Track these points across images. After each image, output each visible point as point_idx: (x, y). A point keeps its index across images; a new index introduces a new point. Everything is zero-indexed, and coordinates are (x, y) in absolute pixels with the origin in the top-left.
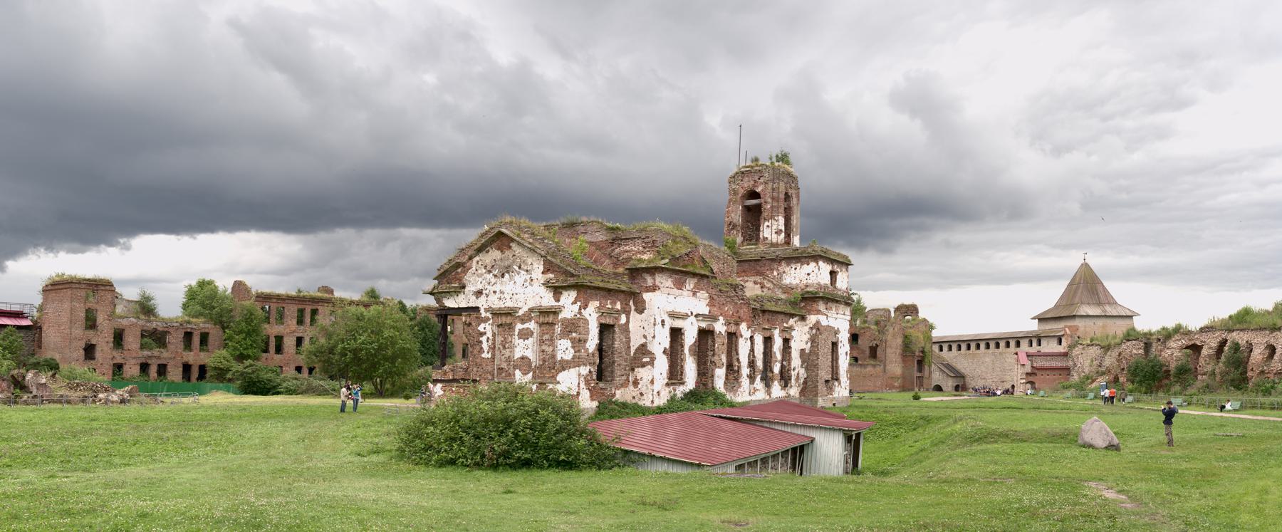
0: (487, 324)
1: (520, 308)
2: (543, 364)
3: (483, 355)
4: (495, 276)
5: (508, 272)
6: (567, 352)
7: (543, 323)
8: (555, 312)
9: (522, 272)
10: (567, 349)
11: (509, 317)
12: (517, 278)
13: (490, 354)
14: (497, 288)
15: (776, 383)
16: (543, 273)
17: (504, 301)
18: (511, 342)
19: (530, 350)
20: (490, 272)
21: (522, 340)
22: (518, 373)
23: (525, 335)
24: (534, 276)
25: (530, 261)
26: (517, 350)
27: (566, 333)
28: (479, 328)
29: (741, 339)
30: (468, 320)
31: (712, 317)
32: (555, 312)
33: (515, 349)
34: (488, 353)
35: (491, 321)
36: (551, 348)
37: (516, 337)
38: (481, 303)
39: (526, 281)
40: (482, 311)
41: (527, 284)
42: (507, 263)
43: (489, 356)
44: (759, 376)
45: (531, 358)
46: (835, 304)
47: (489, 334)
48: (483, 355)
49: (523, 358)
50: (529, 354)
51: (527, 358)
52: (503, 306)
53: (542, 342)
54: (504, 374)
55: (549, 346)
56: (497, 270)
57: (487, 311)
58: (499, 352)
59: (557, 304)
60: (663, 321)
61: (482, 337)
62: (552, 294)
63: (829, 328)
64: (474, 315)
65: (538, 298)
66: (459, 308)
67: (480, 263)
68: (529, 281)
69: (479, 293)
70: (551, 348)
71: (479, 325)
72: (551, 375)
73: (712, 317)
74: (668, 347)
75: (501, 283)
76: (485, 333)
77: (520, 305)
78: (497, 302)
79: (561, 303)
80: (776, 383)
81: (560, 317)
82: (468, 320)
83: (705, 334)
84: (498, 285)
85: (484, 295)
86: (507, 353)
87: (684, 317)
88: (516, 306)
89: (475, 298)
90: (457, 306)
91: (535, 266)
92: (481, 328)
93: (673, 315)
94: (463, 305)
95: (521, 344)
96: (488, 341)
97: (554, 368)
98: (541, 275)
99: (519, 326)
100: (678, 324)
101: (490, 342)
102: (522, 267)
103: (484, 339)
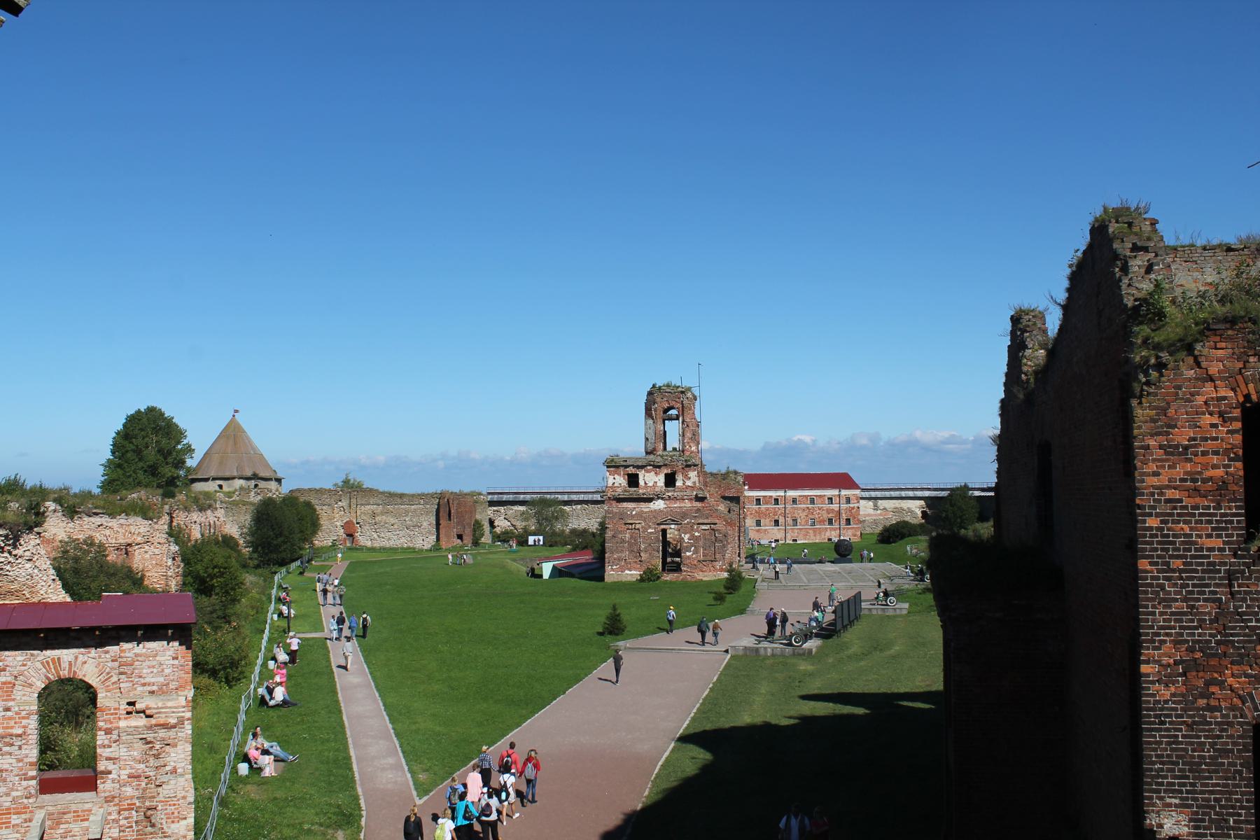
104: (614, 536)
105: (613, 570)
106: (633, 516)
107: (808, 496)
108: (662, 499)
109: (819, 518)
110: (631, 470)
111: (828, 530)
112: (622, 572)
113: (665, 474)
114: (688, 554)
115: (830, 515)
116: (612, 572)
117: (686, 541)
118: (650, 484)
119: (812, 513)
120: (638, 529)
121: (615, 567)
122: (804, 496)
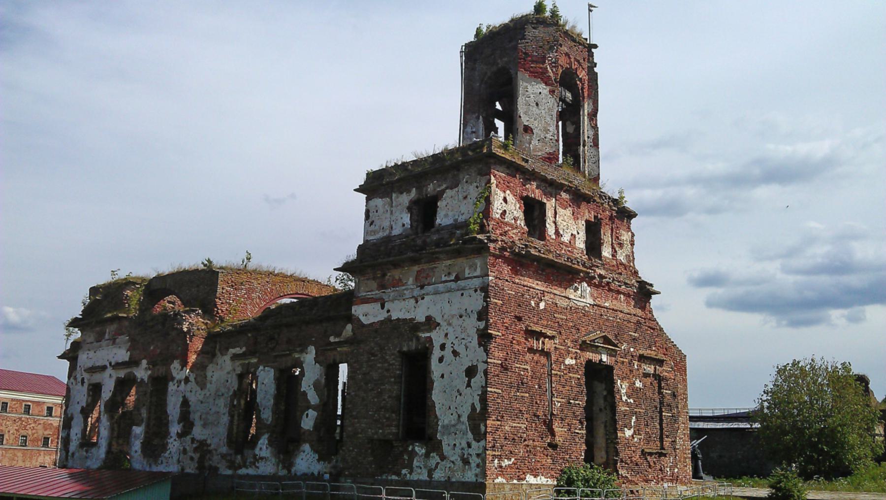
15: (306, 447)
29: (171, 383)
31: (133, 362)
44: (266, 436)
46: (416, 268)
60: (83, 379)
63: (391, 326)
73: (133, 362)
74: (85, 406)
80: (306, 447)
83: (123, 385)
87: (104, 368)
93: (92, 370)
100: (96, 378)
104: (504, 368)
105: (501, 470)
106: (540, 314)
107: (24, 401)
108: (590, 280)
109: (33, 434)
110: (534, 191)
111: (42, 453)
112: (519, 479)
113: (587, 222)
114: (628, 433)
115: (46, 433)
116: (500, 480)
117: (624, 398)
118: (566, 238)
119: (25, 426)
120: (547, 354)
121: (506, 463)
122: (18, 400)
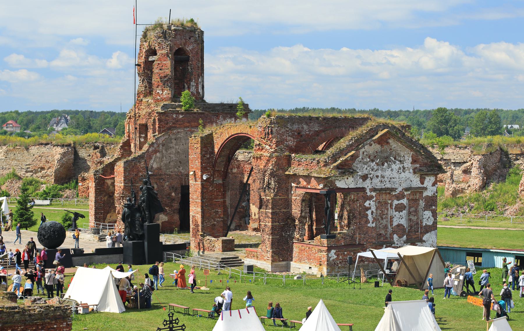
0: (371, 201)
1: (396, 189)
2: (410, 229)
3: (369, 225)
4: (377, 164)
5: (387, 162)
6: (429, 220)
7: (412, 200)
8: (420, 190)
9: (397, 162)
10: (429, 217)
11: (388, 196)
12: (393, 166)
13: (374, 224)
14: (379, 173)
16: (411, 163)
17: (385, 183)
18: (387, 214)
19: (403, 220)
20: (373, 161)
21: (397, 212)
22: (395, 237)
23: (400, 208)
24: (406, 165)
25: (402, 154)
26: (395, 220)
27: (426, 208)
28: (365, 204)
30: (356, 198)
32: (420, 190)
33: (393, 219)
34: (373, 223)
35: (374, 199)
36: (416, 218)
37: (394, 210)
38: (367, 185)
39: (400, 168)
40: (368, 191)
41: (401, 171)
42: (385, 155)
43: (374, 225)
45: (405, 225)
47: (373, 209)
48: (369, 225)
49: (399, 225)
50: (403, 222)
51: (402, 225)
52: (384, 187)
53: (409, 213)
54: (382, 239)
55: (414, 215)
56: (379, 160)
57: (371, 190)
58: (378, 222)
59: (422, 186)
61: (367, 210)
62: (418, 179)
64: (361, 194)
65: (408, 181)
66: (348, 188)
67: (365, 154)
68: (402, 169)
69: (365, 178)
70: (416, 218)
71: (365, 202)
72: (416, 236)
75: (382, 170)
76: (370, 208)
77: (396, 186)
78: (379, 184)
79: (425, 185)
81: (425, 194)
82: (356, 198)
84: (380, 172)
85: (369, 178)
86: (384, 222)
88: (393, 187)
89: (361, 180)
90: (347, 187)
91: (406, 158)
92: (367, 204)
94: (352, 186)
95: (397, 216)
96: (372, 214)
97: (418, 232)
98: (410, 165)
99: (396, 202)
101: (374, 214)
102: (397, 158)
103: (369, 212)
